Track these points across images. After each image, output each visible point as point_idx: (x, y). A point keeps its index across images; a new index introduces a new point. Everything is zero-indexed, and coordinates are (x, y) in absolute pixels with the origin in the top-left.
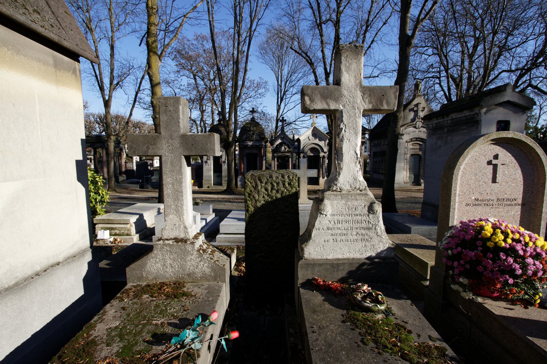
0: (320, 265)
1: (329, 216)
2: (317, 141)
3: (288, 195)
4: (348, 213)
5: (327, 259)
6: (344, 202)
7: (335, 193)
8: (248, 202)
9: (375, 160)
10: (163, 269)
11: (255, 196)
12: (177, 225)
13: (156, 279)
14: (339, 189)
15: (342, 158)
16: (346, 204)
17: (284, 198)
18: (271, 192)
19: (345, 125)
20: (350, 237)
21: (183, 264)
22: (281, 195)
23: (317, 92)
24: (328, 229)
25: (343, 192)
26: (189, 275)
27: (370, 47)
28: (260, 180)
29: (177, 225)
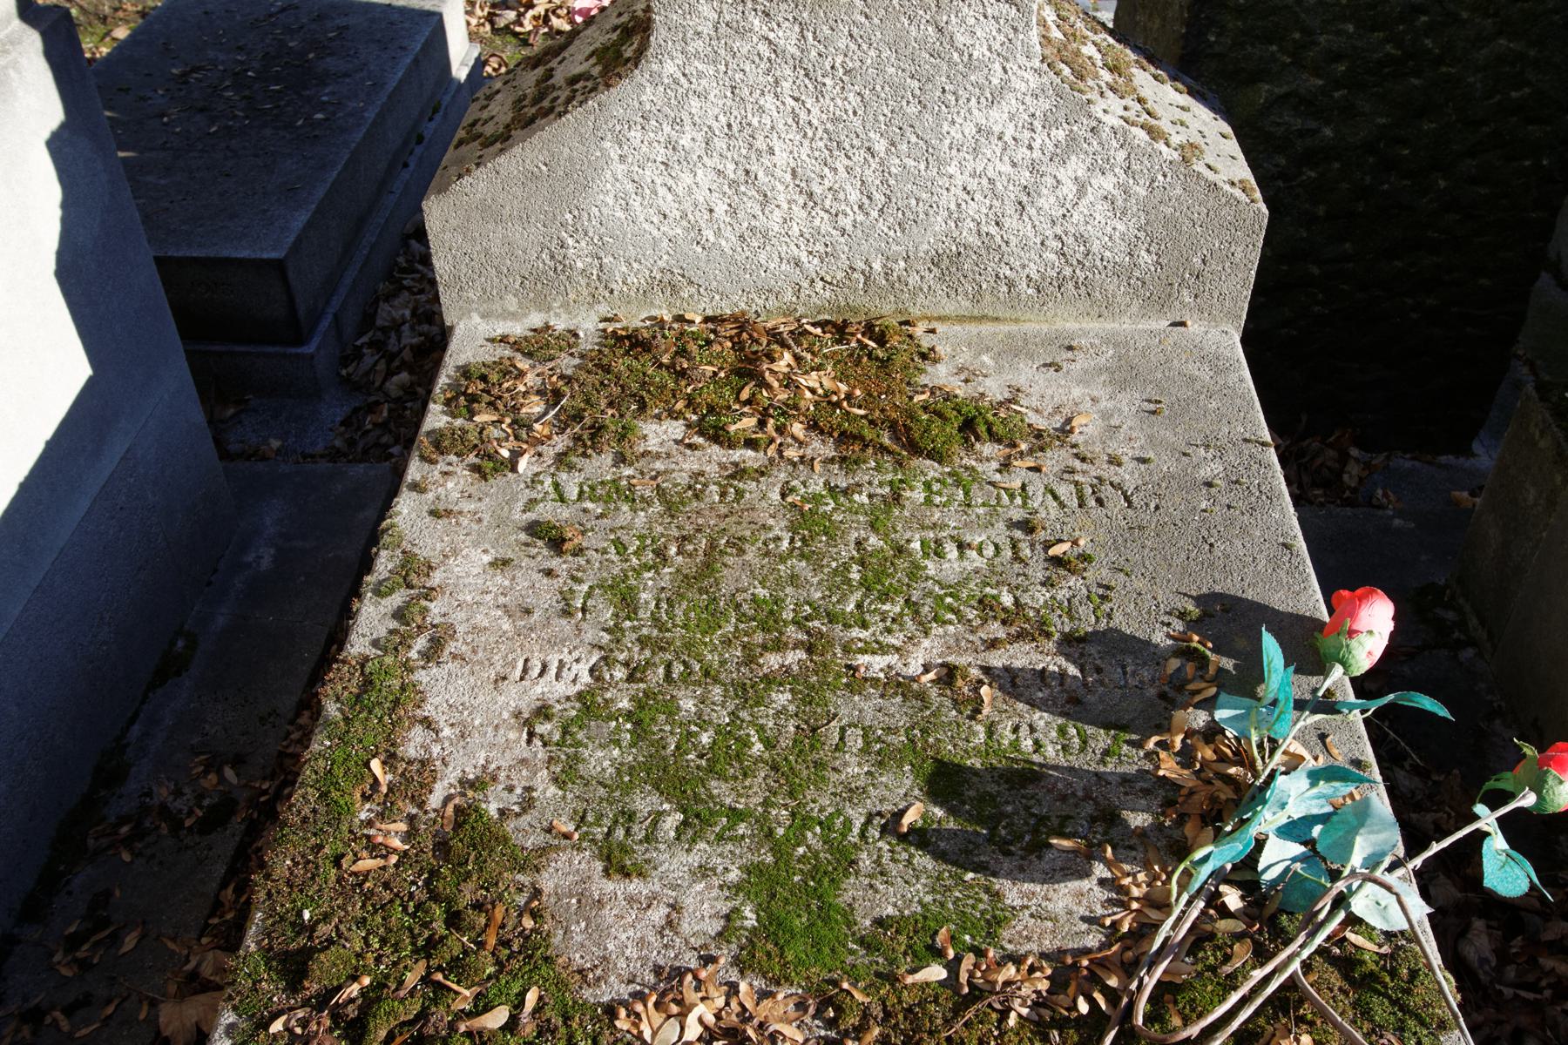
10: (733, 211)
13: (674, 289)
26: (947, 263)
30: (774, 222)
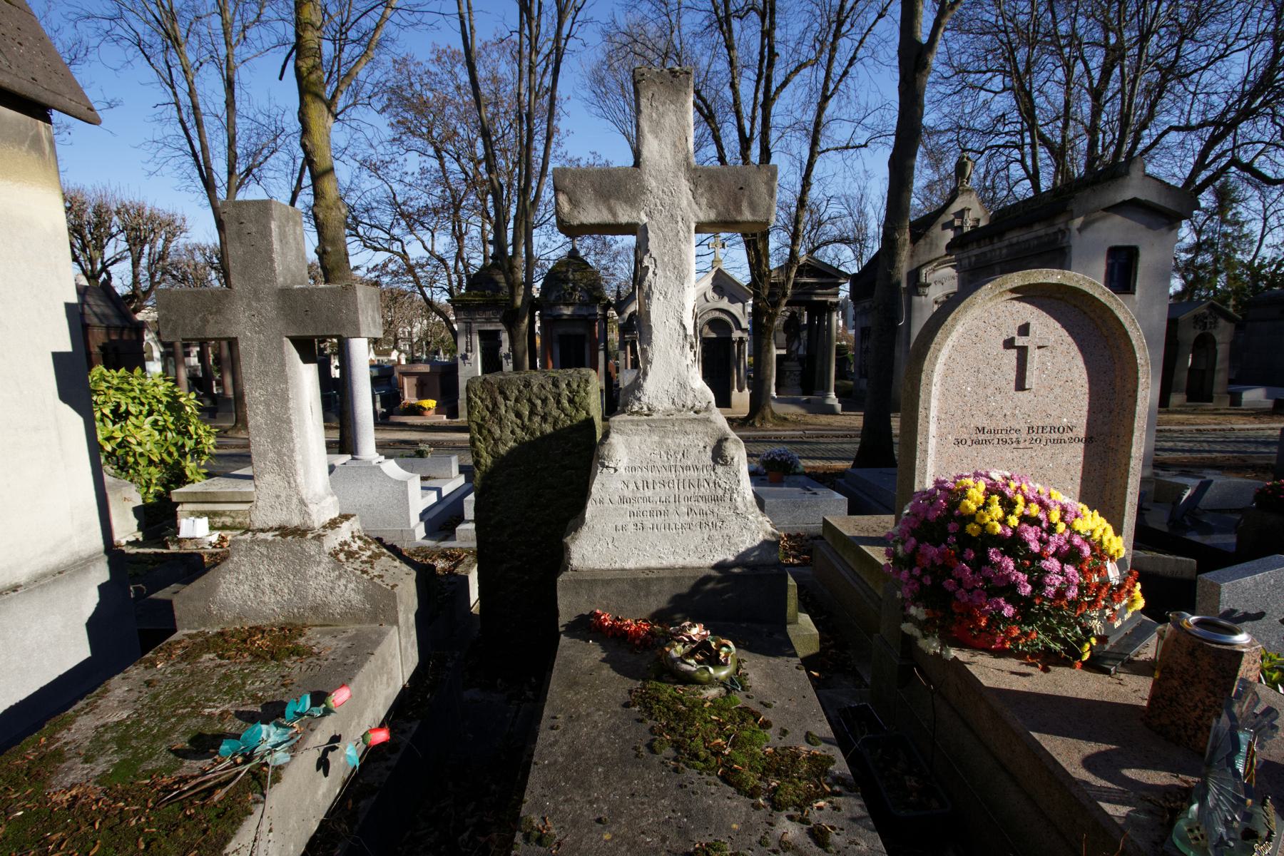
0: (607, 583)
2: (725, 303)
3: (570, 427)
4: (666, 464)
5: (623, 570)
6: (656, 438)
7: (636, 418)
8: (478, 444)
9: (864, 347)
10: (255, 596)
11: (493, 430)
12: (283, 498)
13: (241, 619)
14: (645, 408)
16: (660, 444)
18: (530, 419)
19: (655, 260)
20: (674, 519)
21: (299, 585)
22: (554, 428)
25: (655, 416)
26: (315, 609)
27: (845, 73)
29: (283, 498)
30: (267, 599)
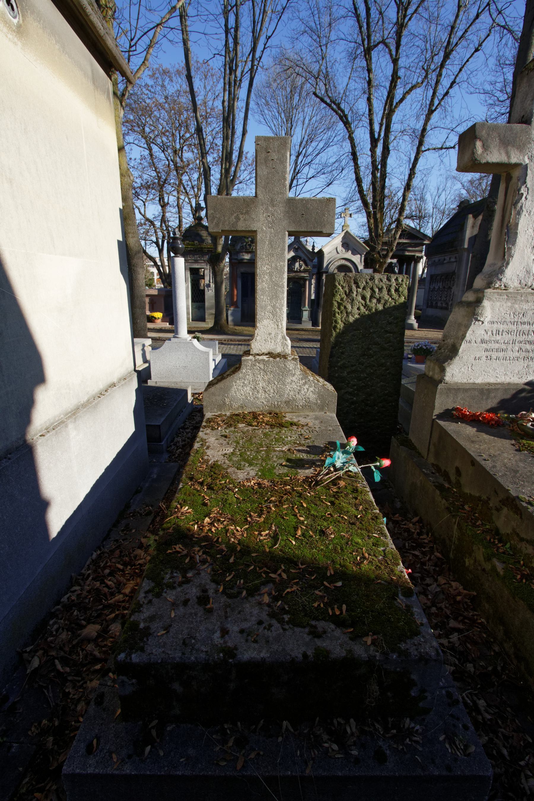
0: (466, 390)
1: (486, 323)
2: (349, 255)
3: (394, 306)
4: (512, 320)
5: (474, 384)
6: (509, 304)
7: (498, 291)
8: (337, 315)
9: (432, 287)
10: (253, 394)
11: (347, 307)
12: (273, 335)
13: (243, 407)
14: (503, 286)
15: (516, 241)
16: (511, 307)
17: (386, 311)
18: (370, 301)
19: (528, 189)
20: (510, 354)
21: (280, 388)
22: (384, 307)
23: (495, 134)
24: (483, 341)
25: (511, 290)
26: (287, 403)
27: (447, 93)
28: (356, 283)
29: (273, 335)
30: (259, 396)
